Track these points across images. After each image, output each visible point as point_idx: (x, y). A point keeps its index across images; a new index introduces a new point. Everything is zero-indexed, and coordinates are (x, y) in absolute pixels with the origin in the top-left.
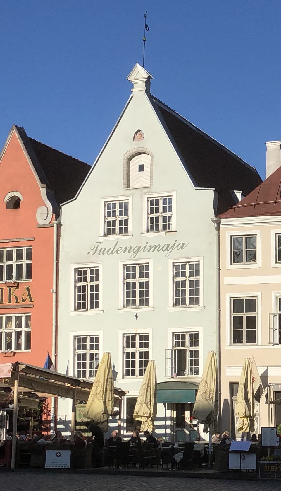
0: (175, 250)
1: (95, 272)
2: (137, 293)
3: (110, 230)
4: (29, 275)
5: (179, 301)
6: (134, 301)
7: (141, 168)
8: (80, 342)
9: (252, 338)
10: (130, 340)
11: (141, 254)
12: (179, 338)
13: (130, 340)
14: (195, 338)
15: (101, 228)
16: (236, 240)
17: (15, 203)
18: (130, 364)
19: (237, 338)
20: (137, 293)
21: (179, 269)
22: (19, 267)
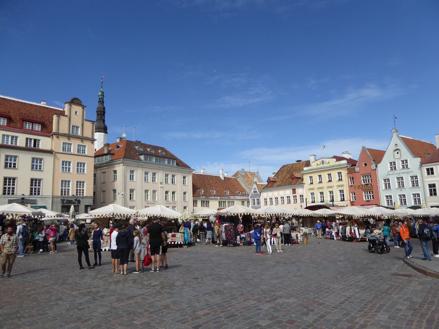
1: (388, 179)
2: (401, 184)
3: (392, 169)
7: (398, 153)
8: (387, 197)
10: (400, 196)
11: (400, 174)
12: (414, 195)
13: (400, 196)
14: (418, 195)
15: (389, 169)
16: (428, 170)
17: (366, 165)
19: (431, 195)
20: (401, 184)
21: (412, 177)
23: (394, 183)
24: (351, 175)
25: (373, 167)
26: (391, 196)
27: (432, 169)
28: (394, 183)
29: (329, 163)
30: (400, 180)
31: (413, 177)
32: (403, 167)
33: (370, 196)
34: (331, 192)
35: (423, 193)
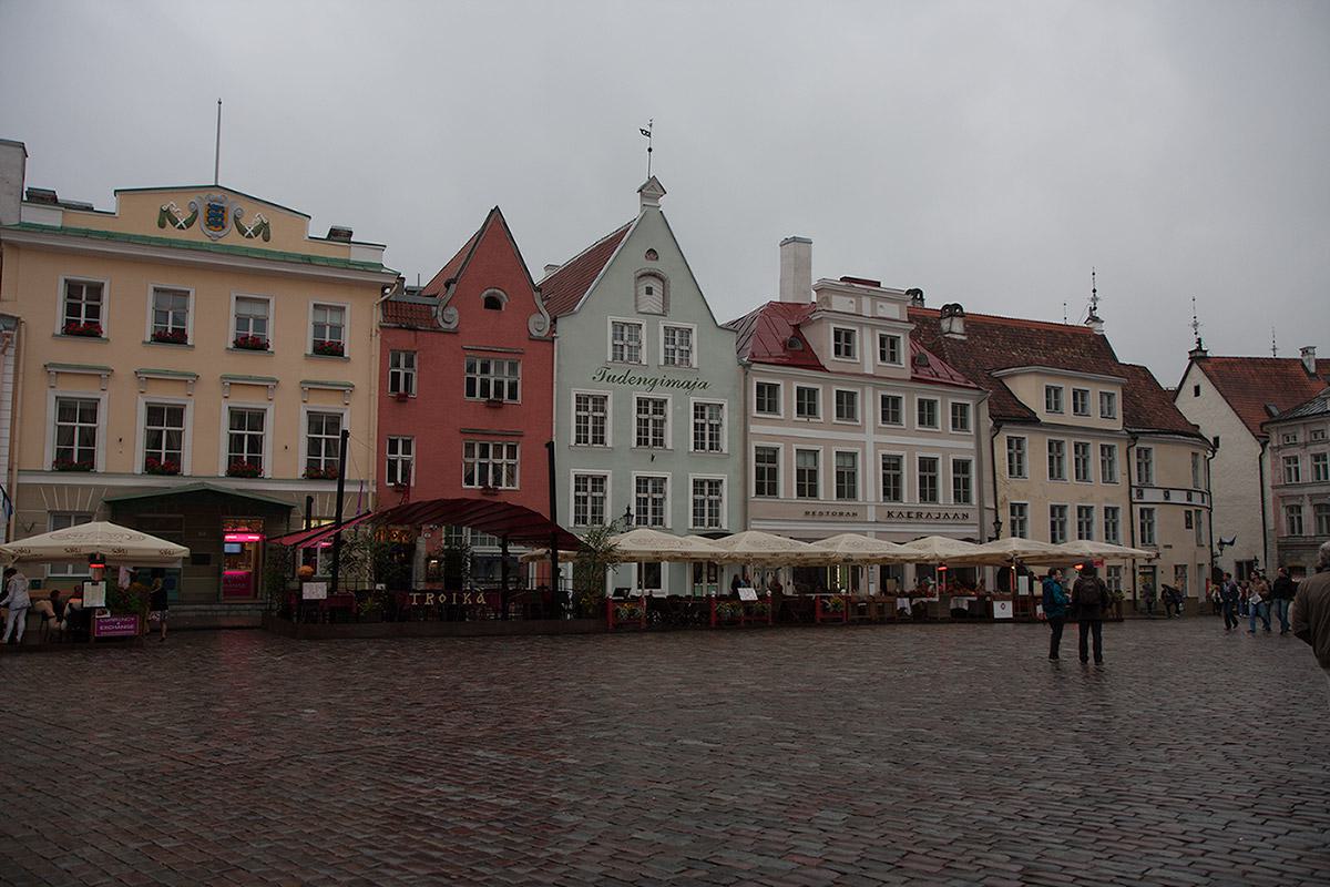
0: (696, 390)
1: (600, 402)
2: (650, 434)
4: (513, 395)
5: (699, 445)
6: (647, 441)
7: (649, 291)
9: (773, 491)
12: (698, 484)
14: (715, 485)
16: (760, 387)
17: (492, 303)
18: (642, 510)
19: (759, 491)
20: (650, 434)
21: (699, 409)
22: (499, 385)
23: (621, 424)
24: (405, 340)
25: (538, 324)
26: (599, 481)
27: (773, 388)
28: (621, 424)
29: (263, 230)
30: (651, 410)
31: (703, 409)
32: (669, 361)
33: (497, 469)
34: (247, 424)
35: (739, 478)
